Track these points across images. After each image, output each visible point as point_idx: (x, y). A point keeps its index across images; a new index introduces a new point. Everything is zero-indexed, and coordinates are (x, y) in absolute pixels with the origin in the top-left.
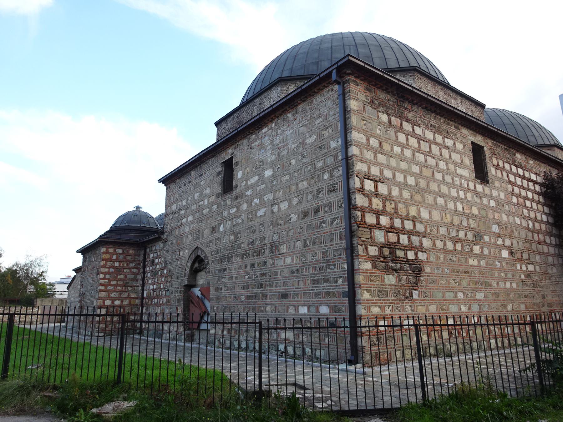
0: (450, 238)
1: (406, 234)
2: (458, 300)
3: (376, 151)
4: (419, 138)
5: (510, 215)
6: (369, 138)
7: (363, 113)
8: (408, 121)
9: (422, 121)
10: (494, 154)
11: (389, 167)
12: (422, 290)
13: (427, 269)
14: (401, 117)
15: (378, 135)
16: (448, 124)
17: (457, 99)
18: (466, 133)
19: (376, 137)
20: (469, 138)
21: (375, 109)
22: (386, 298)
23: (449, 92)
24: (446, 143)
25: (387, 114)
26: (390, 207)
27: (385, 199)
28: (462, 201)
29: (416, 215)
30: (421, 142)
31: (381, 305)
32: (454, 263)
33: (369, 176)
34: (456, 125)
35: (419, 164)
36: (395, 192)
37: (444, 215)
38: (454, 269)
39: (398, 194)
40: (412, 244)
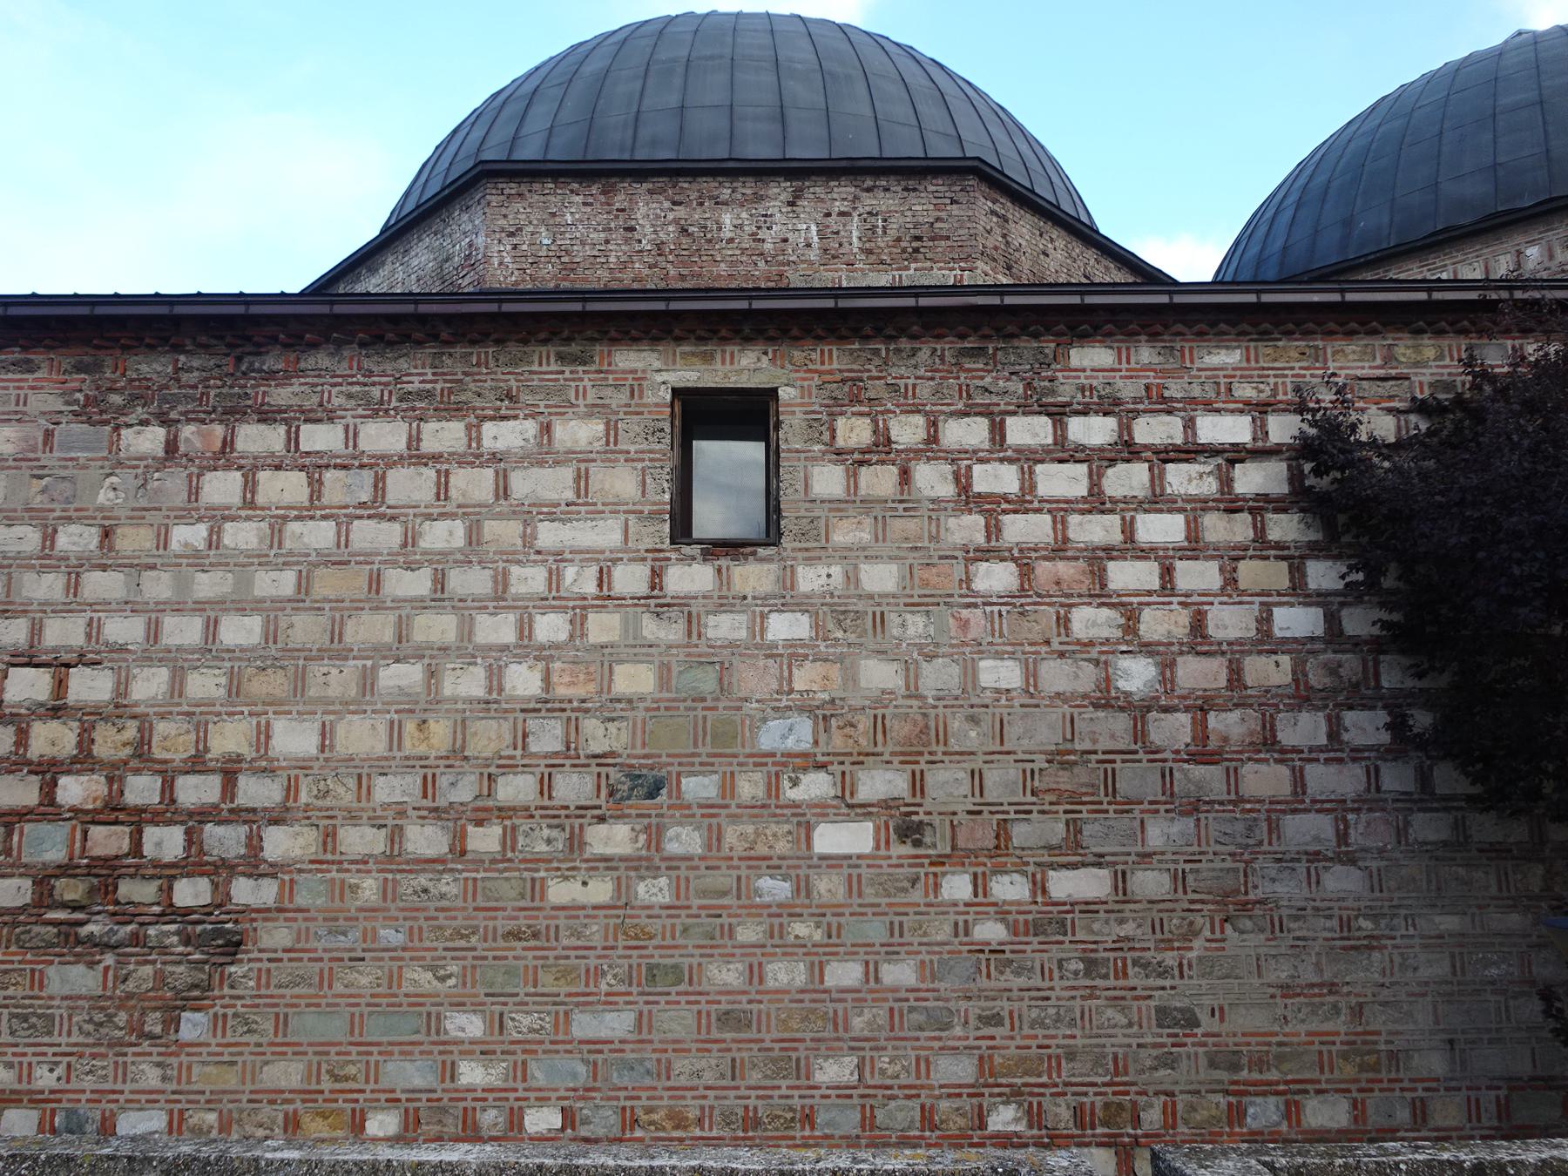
0: (436, 810)
1: (182, 823)
2: (444, 1043)
3: (82, 566)
4: (324, 461)
5: (930, 657)
6: (55, 531)
7: (39, 454)
8: (266, 416)
9: (350, 396)
10: (855, 400)
11: (130, 607)
12: (230, 1012)
13: (277, 936)
14: (233, 414)
15: (101, 509)
16: (514, 362)
17: (759, 198)
18: (640, 365)
19: (86, 518)
20: (659, 378)
21: (106, 423)
22: (46, 1040)
23: (707, 185)
24: (487, 443)
25: (165, 421)
26: (109, 743)
27: (89, 718)
28: (544, 655)
29: (247, 752)
30: (329, 476)
31: (16, 1060)
32: (444, 903)
33: (31, 657)
34: (574, 348)
35: (298, 563)
36: (149, 685)
37: (410, 726)
38: (440, 928)
39: (164, 688)
40: (201, 852)
